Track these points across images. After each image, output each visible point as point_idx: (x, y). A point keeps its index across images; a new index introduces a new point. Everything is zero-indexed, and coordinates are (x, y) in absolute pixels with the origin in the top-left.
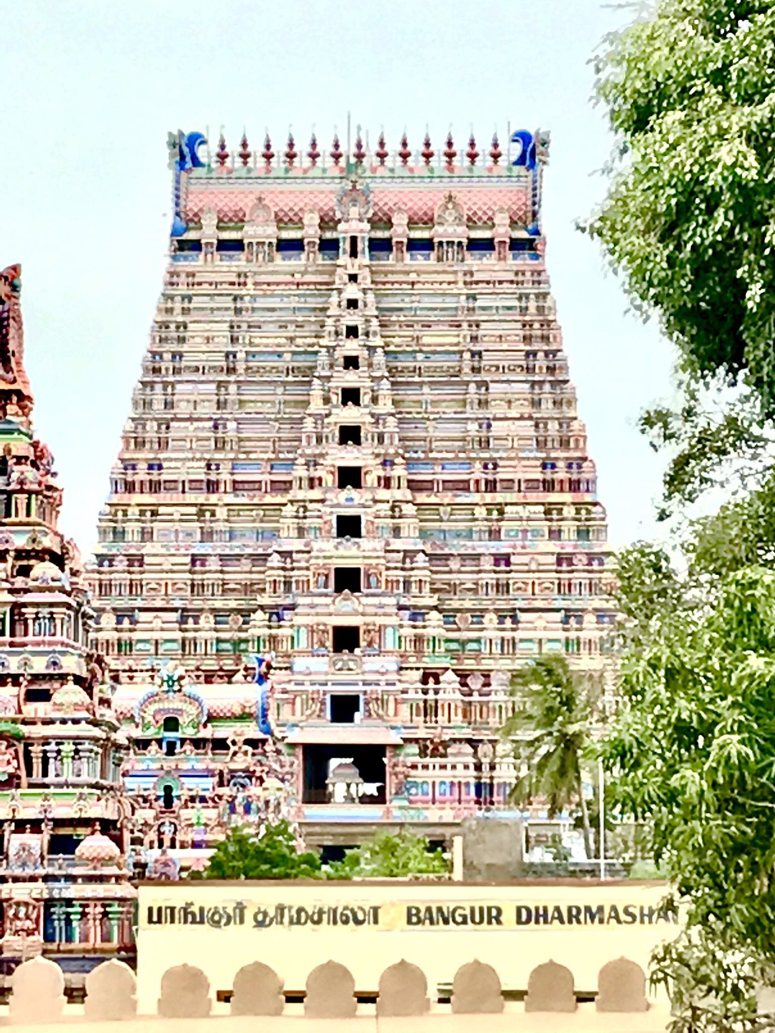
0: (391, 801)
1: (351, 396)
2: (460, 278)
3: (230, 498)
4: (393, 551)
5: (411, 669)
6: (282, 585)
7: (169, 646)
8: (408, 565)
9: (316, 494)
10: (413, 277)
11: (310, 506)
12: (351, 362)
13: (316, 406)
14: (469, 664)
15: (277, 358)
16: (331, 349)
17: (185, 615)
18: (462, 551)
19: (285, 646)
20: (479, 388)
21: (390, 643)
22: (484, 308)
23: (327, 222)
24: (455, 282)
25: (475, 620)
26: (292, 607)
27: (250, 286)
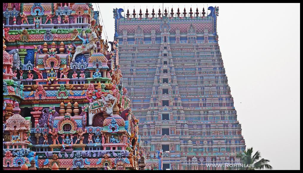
1: (165, 81)
2: (195, 48)
4: (178, 124)
6: (147, 133)
8: (182, 127)
10: (182, 47)
11: (155, 111)
12: (165, 71)
13: (156, 84)
14: (200, 155)
15: (144, 70)
16: (160, 68)
18: (197, 123)
19: (149, 150)
20: (201, 78)
21: (178, 149)
22: (202, 56)
23: (158, 32)
24: (193, 49)
25: (201, 142)
26: (150, 140)
27: (137, 50)
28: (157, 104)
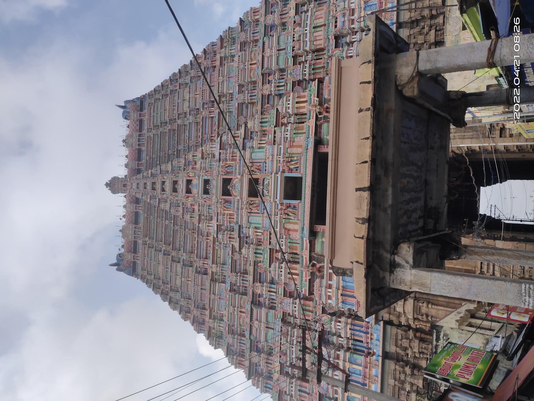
3: (210, 262)
5: (275, 137)
9: (196, 208)
17: (256, 302)
28: (191, 205)
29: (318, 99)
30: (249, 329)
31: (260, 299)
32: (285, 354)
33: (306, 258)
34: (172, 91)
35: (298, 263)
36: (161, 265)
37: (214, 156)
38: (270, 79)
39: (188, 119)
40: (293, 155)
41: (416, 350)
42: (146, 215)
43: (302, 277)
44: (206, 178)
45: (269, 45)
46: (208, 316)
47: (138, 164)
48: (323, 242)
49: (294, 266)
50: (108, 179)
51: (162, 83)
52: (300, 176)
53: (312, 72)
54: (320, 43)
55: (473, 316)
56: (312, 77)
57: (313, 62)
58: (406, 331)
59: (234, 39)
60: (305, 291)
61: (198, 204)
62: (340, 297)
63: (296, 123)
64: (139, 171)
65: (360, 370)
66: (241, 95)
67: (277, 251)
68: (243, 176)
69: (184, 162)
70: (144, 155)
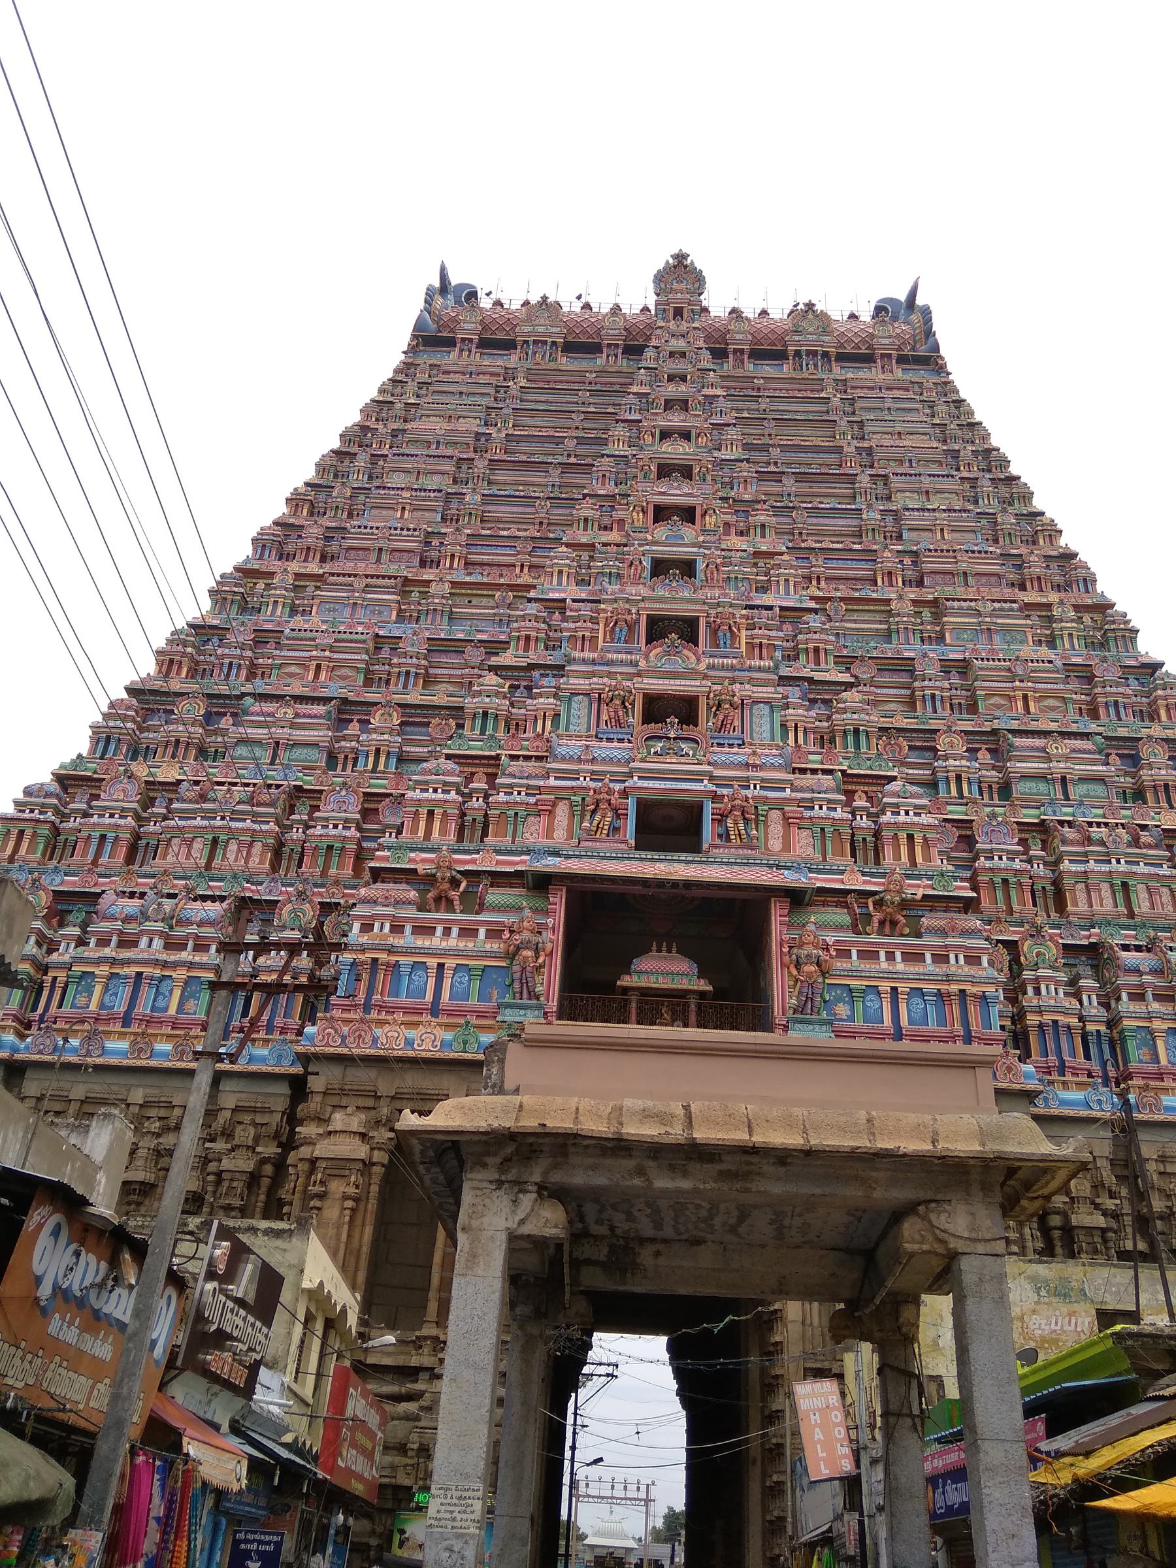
0: (786, 1028)
5: (814, 771)
7: (300, 753)
17: (346, 712)
26: (559, 670)
28: (621, 522)
29: (919, 897)
30: (269, 690)
31: (355, 723)
32: (203, 798)
33: (474, 861)
34: (955, 455)
35: (460, 839)
36: (446, 426)
37: (763, 589)
38: (979, 755)
39: (870, 506)
40: (761, 826)
41: (226, 1164)
42: (591, 376)
43: (422, 850)
44: (701, 566)
45: (1080, 751)
46: (302, 571)
47: (742, 351)
48: (520, 909)
49: (453, 828)
50: (698, 260)
51: (980, 423)
52: (705, 846)
53: (998, 879)
54: (1078, 903)
55: (329, 1324)
56: (983, 878)
57: (1026, 880)
58: (277, 1135)
59: (1103, 645)
60: (384, 859)
61: (624, 541)
62: (369, 955)
63: (853, 835)
64: (719, 354)
65: (166, 1009)
66: (938, 666)
67: (492, 777)
68: (706, 677)
69: (747, 497)
70: (768, 369)
